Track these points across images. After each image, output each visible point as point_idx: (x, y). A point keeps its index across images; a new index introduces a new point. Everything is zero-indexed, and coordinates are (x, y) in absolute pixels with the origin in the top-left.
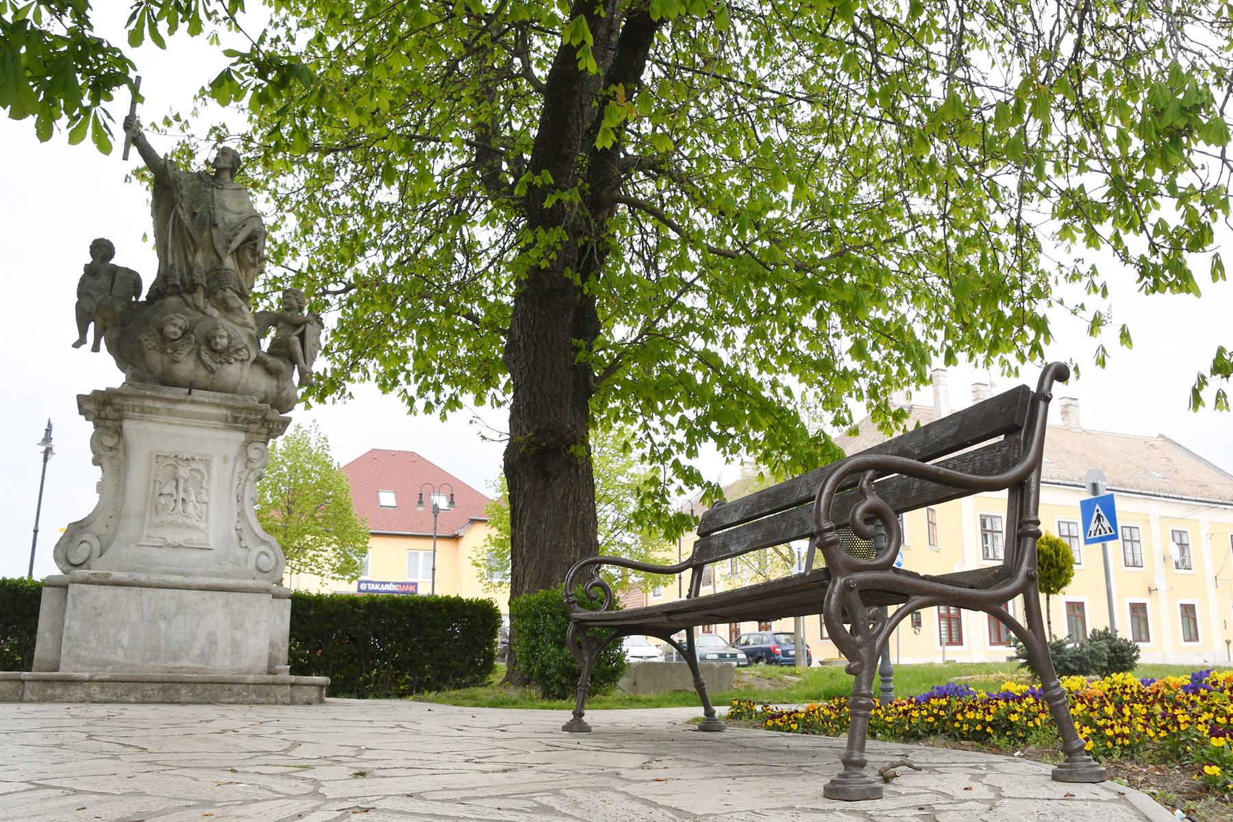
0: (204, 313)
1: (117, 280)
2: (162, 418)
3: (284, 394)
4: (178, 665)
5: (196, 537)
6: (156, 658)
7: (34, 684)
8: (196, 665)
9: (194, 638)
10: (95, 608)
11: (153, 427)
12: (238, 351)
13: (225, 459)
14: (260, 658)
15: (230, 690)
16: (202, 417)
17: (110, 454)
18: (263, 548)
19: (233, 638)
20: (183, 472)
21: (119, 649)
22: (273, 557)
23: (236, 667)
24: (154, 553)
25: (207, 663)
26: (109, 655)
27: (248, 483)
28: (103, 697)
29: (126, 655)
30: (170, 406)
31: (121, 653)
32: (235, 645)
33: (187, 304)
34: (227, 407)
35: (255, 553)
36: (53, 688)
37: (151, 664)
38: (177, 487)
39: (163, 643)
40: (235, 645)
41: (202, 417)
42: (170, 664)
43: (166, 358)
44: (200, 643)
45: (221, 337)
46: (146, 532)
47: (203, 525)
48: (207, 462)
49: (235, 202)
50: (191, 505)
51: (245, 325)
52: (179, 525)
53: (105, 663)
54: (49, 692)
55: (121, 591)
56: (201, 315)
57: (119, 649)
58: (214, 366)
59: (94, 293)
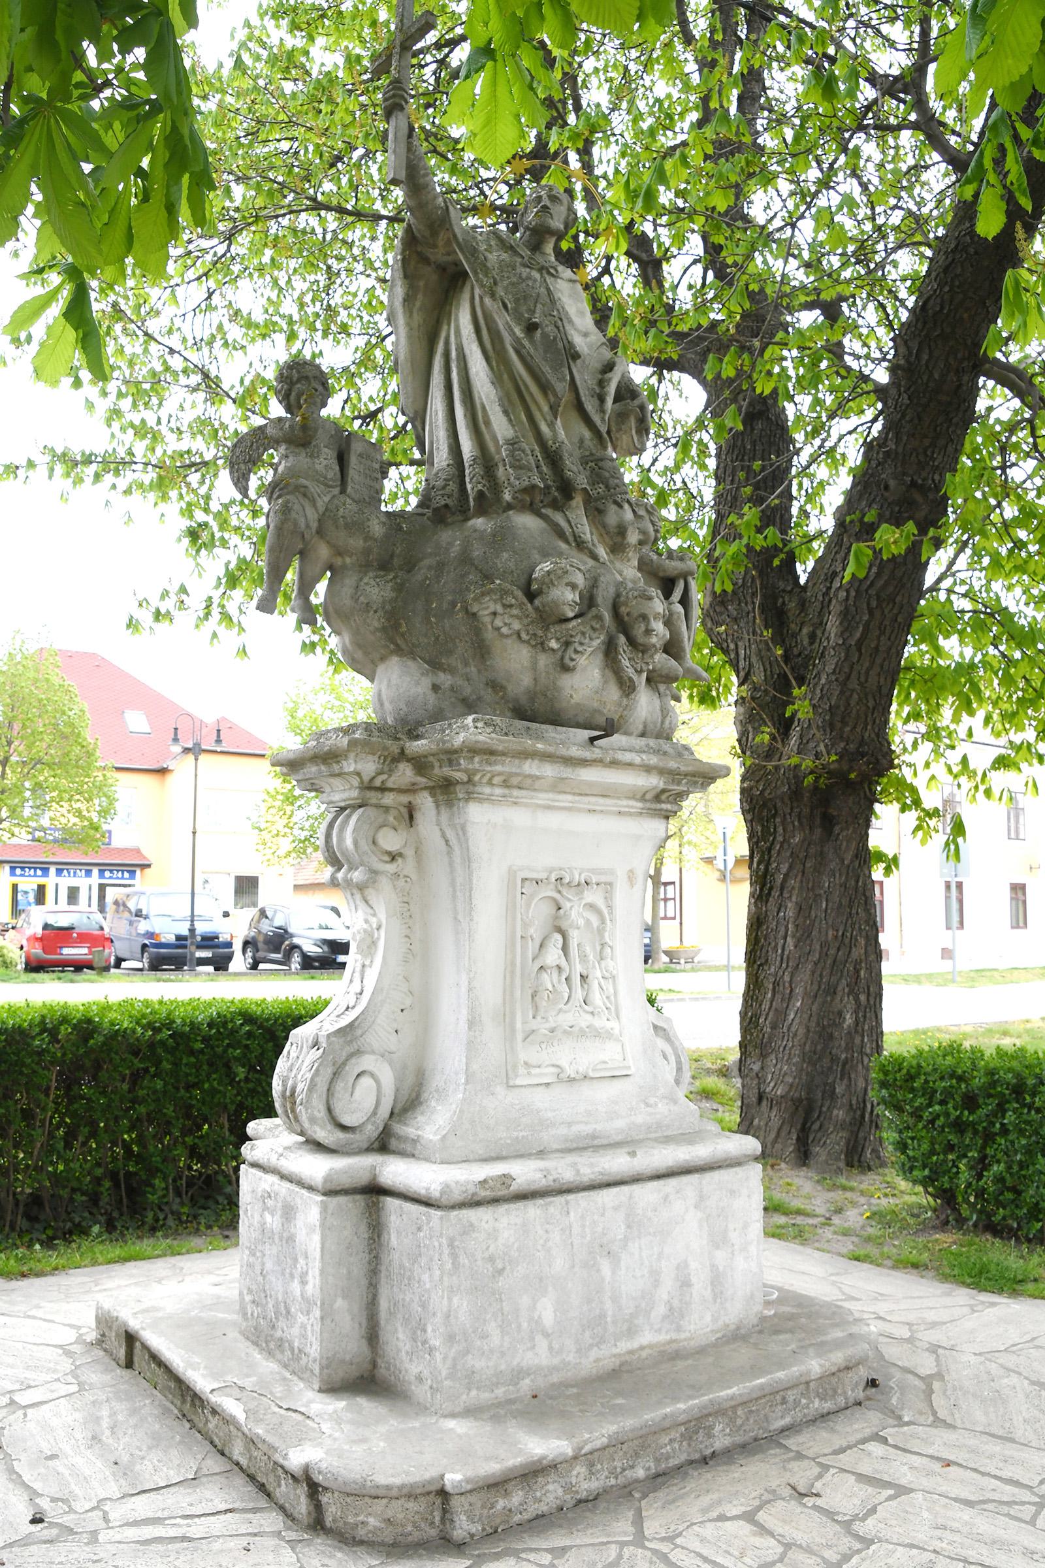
1: (353, 460)
2: (543, 798)
4: (635, 1345)
5: (606, 1054)
6: (601, 1341)
7: (472, 1499)
8: (663, 1337)
9: (656, 1284)
10: (491, 1259)
11: (519, 817)
14: (752, 1296)
16: (606, 792)
17: (391, 868)
19: (713, 1267)
20: (576, 913)
21: (539, 1338)
25: (679, 1329)
26: (528, 1359)
28: (594, 1485)
29: (550, 1348)
30: (567, 772)
31: (542, 1344)
32: (717, 1280)
33: (561, 534)
36: (507, 1494)
37: (594, 1354)
38: (565, 948)
39: (608, 1305)
40: (717, 1280)
41: (606, 792)
42: (624, 1346)
43: (544, 660)
44: (666, 1289)
46: (523, 1056)
52: (582, 1034)
53: (519, 1374)
54: (501, 1503)
55: (532, 1210)
57: (539, 1338)
59: (314, 488)
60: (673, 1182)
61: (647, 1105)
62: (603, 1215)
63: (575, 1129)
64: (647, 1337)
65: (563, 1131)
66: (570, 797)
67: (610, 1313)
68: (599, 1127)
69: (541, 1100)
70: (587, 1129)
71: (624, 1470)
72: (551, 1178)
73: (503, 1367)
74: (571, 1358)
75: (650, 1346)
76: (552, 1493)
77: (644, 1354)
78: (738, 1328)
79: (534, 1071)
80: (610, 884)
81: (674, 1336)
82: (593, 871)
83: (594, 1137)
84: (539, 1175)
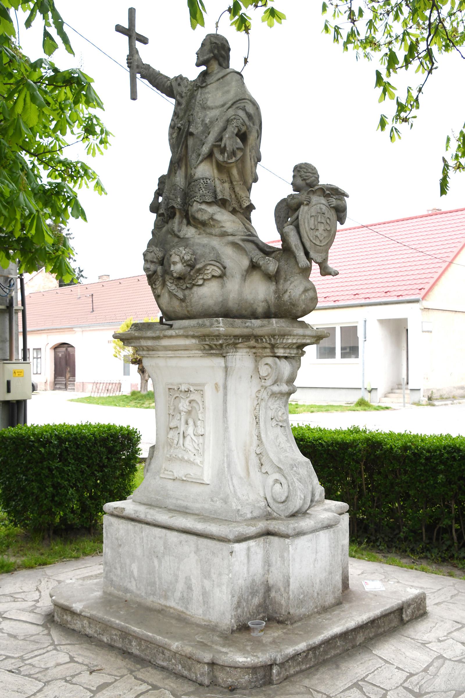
0: (178, 237)
3: (286, 297)
4: (168, 605)
5: (193, 472)
9: (177, 581)
12: (199, 271)
13: (216, 386)
15: (163, 653)
18: (277, 476)
20: (184, 405)
22: (285, 486)
23: (206, 618)
24: (170, 485)
25: (187, 608)
27: (263, 404)
32: (205, 594)
34: (193, 337)
35: (270, 480)
42: (163, 602)
44: (180, 586)
45: (175, 263)
47: (198, 460)
48: (201, 392)
49: (220, 94)
50: (188, 439)
51: (224, 234)
53: (126, 590)
55: (130, 525)
56: (176, 240)
58: (180, 295)
60: (184, 536)
61: (212, 500)
62: (155, 538)
63: (179, 502)
64: (172, 603)
65: (174, 501)
66: (170, 352)
67: (157, 583)
68: (189, 504)
69: (170, 485)
70: (184, 504)
71: (100, 634)
72: (136, 515)
73: (121, 584)
74: (143, 594)
75: (174, 609)
76: (77, 625)
77: (172, 611)
78: (216, 626)
79: (166, 472)
80: (202, 390)
81: (185, 611)
82: (193, 385)
83: (186, 508)
84: (133, 512)
